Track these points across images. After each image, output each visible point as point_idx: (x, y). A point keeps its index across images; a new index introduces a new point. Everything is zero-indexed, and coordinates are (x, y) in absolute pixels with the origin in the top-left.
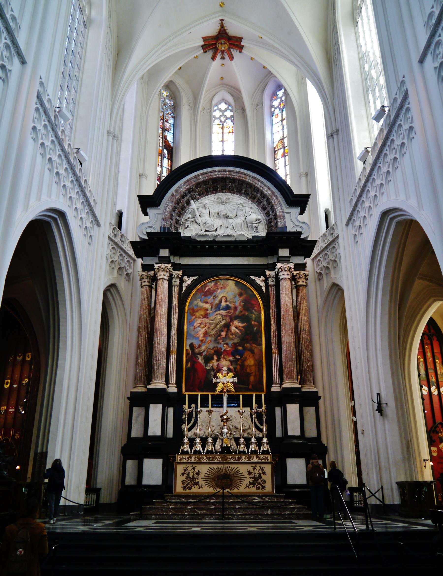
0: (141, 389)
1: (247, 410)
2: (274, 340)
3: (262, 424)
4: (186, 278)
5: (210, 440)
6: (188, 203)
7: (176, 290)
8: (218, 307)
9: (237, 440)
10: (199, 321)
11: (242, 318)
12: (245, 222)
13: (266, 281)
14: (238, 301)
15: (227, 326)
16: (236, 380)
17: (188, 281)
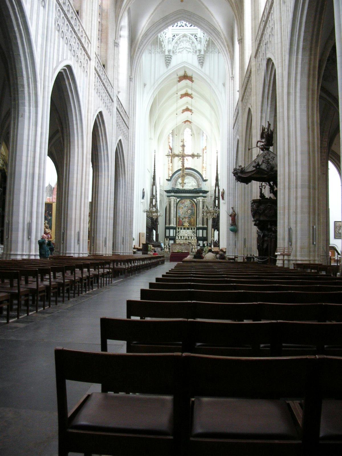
0: (167, 226)
1: (191, 230)
2: (198, 215)
3: (194, 233)
4: (178, 199)
5: (183, 237)
6: (178, 179)
7: (175, 202)
8: (185, 206)
9: (189, 237)
10: (181, 210)
11: (191, 210)
12: (192, 185)
13: (197, 200)
14: (190, 205)
15: (187, 211)
16: (189, 224)
17: (178, 200)
